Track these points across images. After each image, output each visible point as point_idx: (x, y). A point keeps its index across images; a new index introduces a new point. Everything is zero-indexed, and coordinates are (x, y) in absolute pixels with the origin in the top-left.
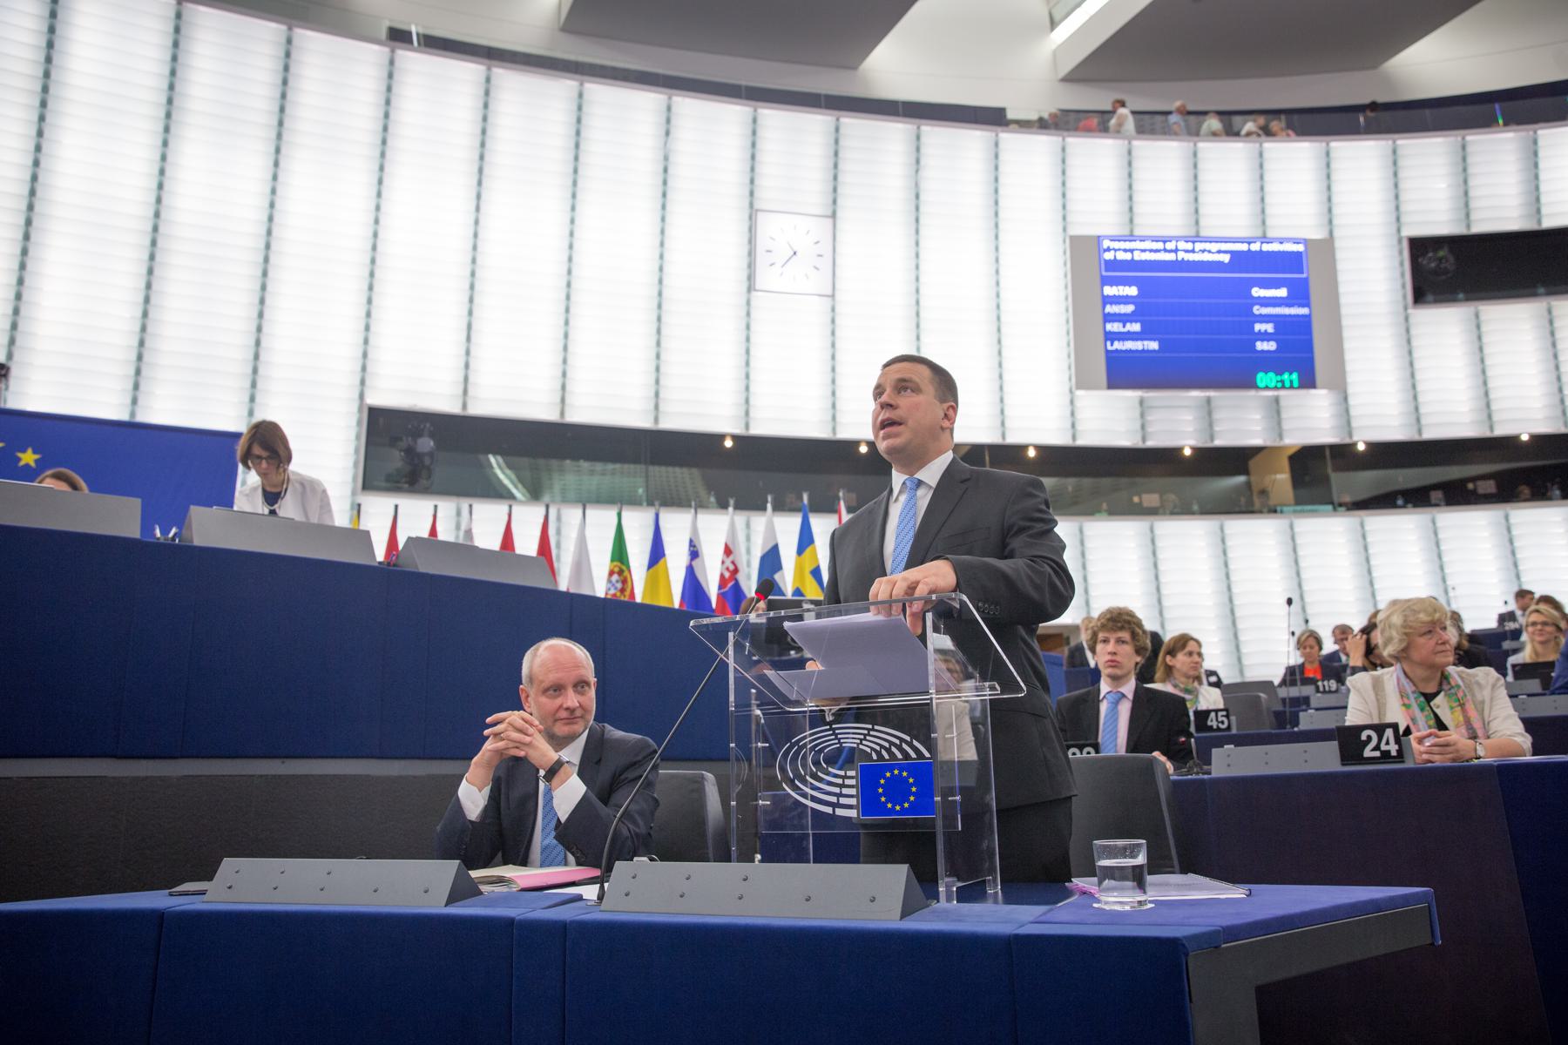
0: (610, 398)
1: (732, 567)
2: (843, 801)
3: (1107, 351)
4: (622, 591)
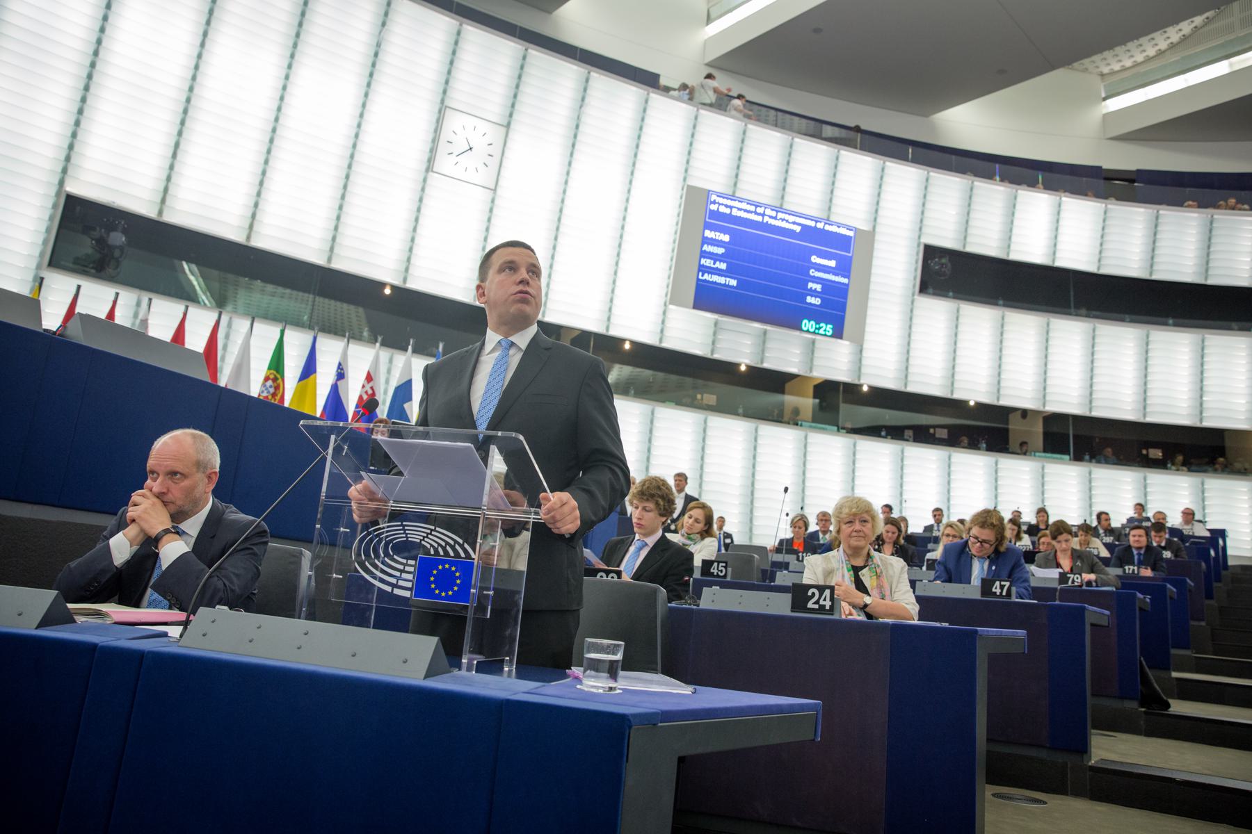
0: (292, 232)
1: (370, 392)
2: (401, 583)
3: (698, 280)
4: (274, 395)
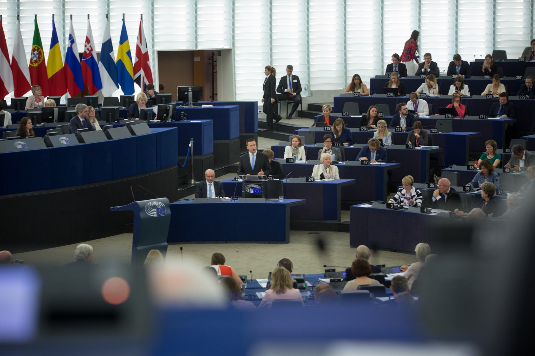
1: (90, 49)
4: (39, 58)
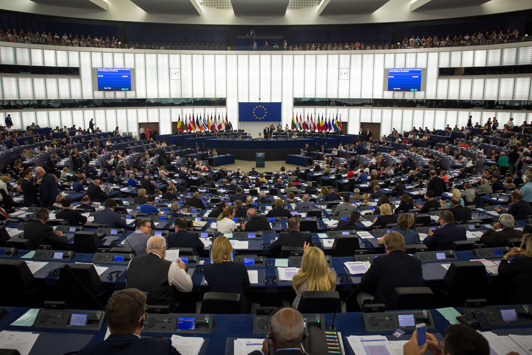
0: (321, 95)
